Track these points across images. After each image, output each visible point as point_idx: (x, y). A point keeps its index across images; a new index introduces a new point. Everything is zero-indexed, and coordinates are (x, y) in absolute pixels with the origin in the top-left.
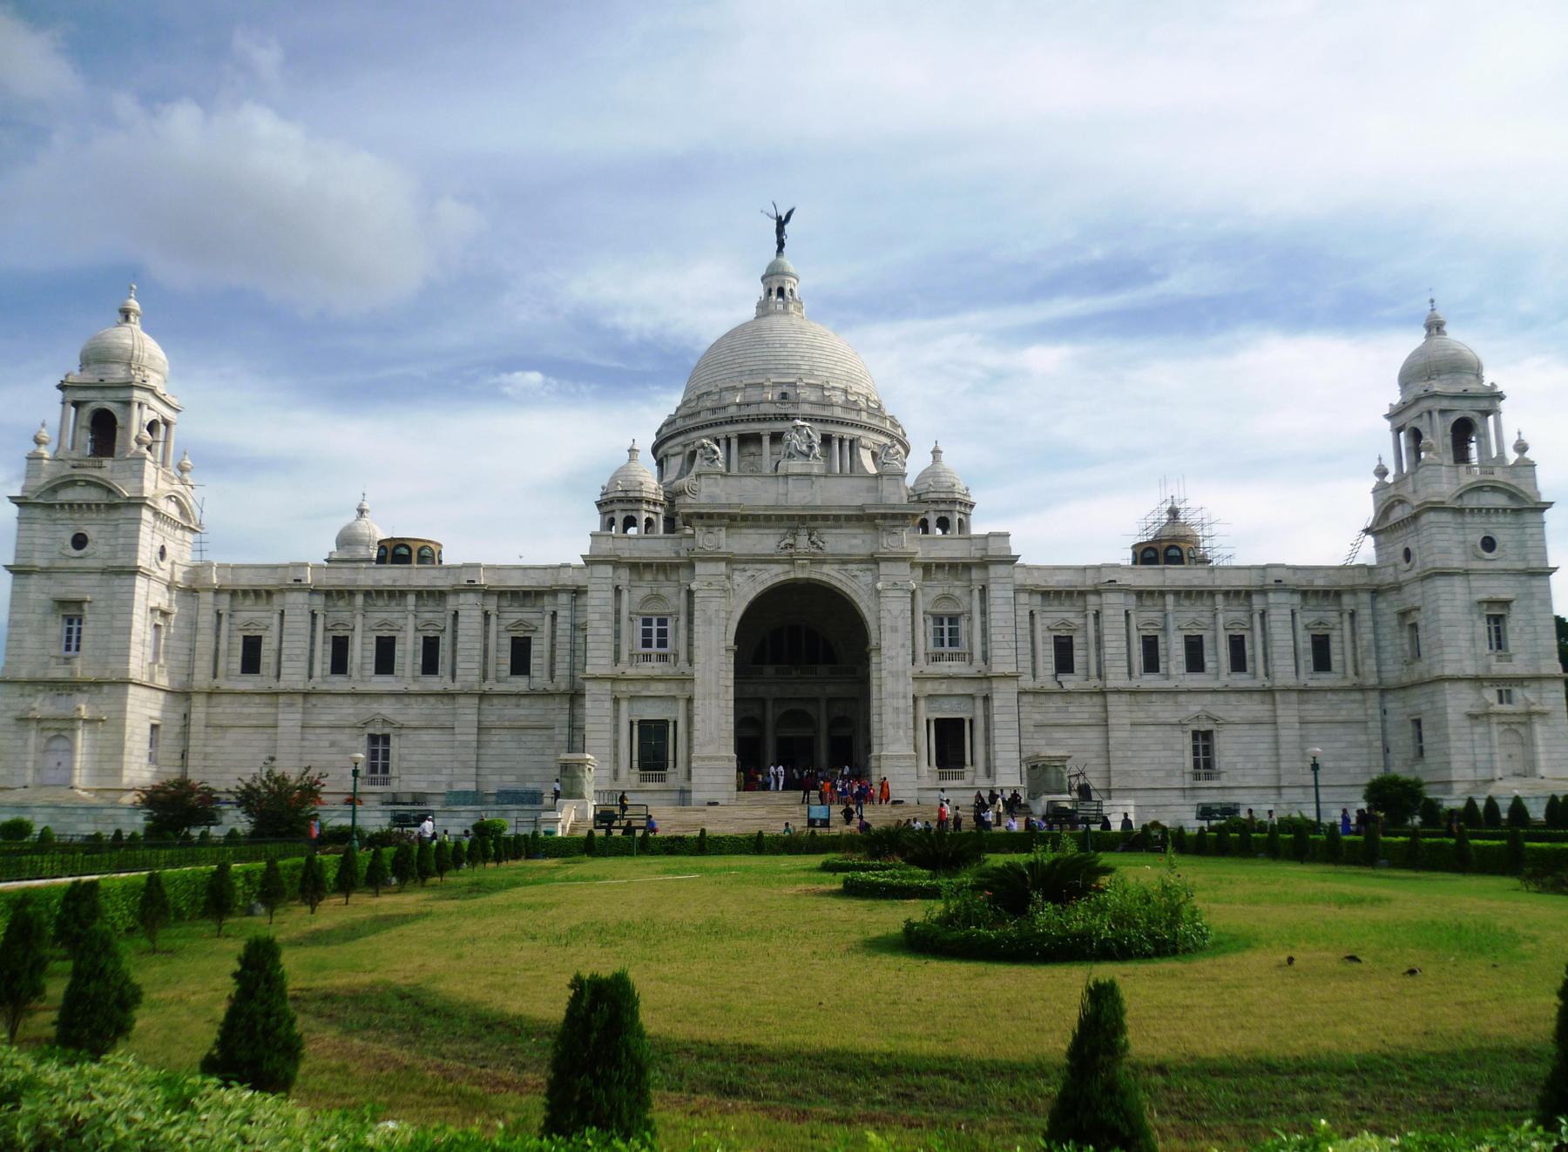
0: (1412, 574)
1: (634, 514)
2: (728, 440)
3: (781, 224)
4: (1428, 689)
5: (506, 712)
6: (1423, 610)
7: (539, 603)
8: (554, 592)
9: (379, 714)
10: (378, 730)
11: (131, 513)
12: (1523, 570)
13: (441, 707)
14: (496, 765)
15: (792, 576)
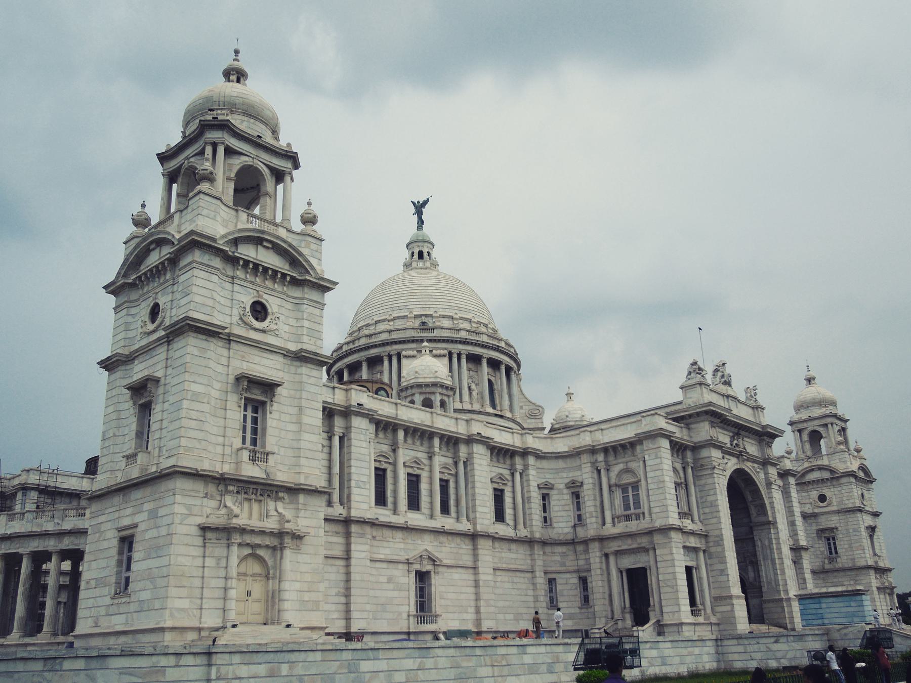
0: (835, 508)
1: (446, 398)
2: (459, 355)
3: (419, 208)
4: (853, 573)
5: (503, 555)
6: (840, 528)
7: (508, 462)
8: (525, 453)
9: (426, 550)
10: (427, 567)
11: (314, 295)
12: (872, 512)
13: (464, 546)
14: (501, 604)
15: (738, 467)
